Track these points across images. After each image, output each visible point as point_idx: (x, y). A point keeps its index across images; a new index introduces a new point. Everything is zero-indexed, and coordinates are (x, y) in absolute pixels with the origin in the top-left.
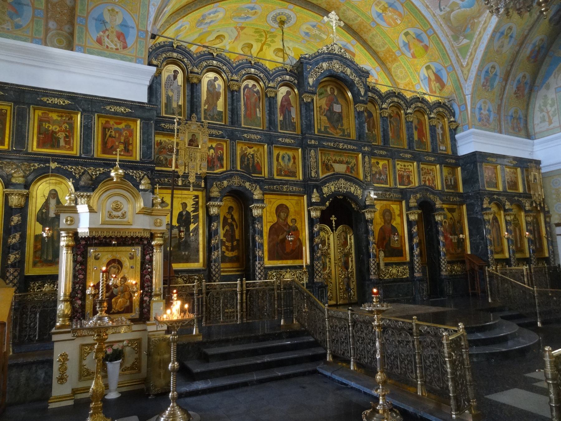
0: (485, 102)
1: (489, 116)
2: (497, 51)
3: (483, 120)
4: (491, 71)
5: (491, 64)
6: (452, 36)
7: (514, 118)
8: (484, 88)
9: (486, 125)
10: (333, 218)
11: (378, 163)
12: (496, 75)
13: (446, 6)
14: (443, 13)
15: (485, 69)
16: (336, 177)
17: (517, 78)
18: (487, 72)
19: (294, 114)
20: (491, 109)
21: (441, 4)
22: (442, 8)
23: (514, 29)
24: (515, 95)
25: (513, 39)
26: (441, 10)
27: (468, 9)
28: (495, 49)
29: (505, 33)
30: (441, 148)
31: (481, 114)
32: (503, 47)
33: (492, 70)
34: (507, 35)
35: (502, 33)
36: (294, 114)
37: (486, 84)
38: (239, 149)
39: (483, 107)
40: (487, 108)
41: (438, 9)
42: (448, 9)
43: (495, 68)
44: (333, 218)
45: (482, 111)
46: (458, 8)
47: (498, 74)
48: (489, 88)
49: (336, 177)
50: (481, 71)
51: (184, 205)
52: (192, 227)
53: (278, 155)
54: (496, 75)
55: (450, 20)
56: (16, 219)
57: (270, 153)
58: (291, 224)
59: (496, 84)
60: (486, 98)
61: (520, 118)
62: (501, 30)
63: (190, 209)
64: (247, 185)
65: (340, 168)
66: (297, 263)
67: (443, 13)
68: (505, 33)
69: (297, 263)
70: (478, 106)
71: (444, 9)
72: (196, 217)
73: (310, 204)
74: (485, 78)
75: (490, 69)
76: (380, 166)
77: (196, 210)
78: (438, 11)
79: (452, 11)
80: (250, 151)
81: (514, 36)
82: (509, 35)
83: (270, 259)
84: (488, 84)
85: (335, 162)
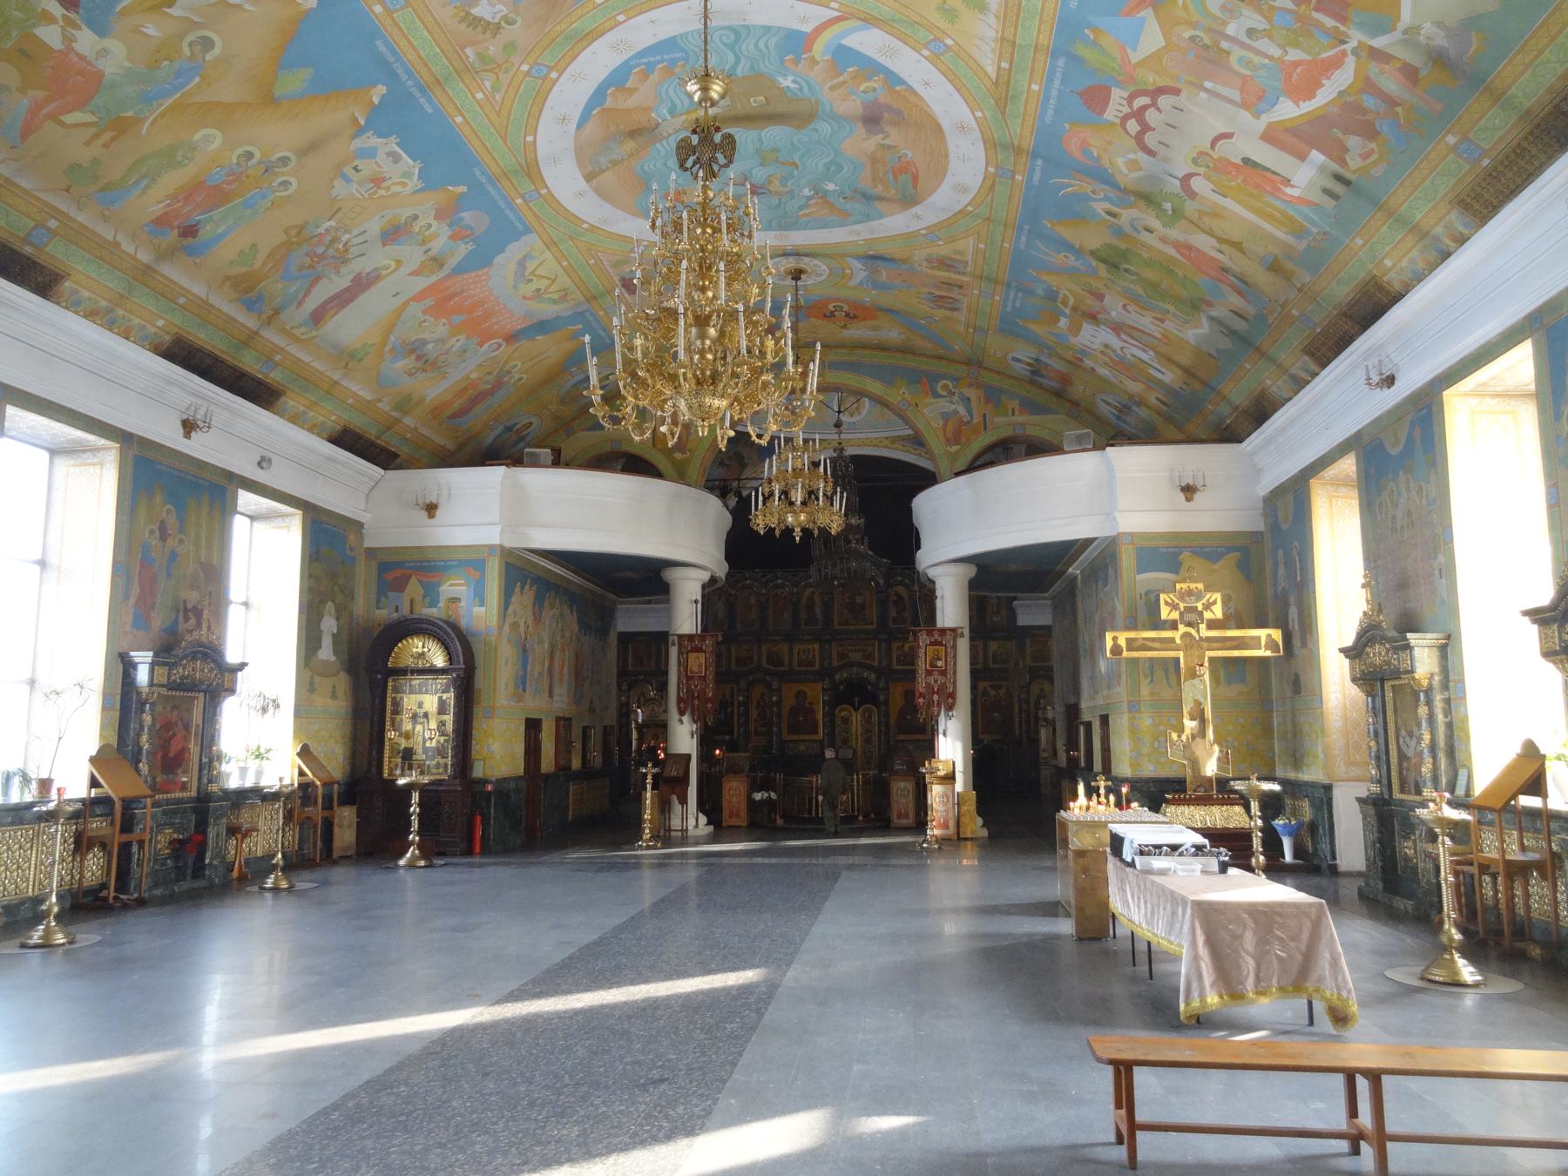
10: (857, 699)
11: (903, 646)
16: (851, 665)
19: (818, 611)
30: (995, 619)
36: (818, 611)
38: (764, 648)
44: (857, 699)
49: (851, 665)
51: (724, 695)
52: (729, 710)
53: (799, 650)
56: (624, 709)
57: (791, 649)
58: (808, 706)
63: (728, 697)
64: (768, 678)
65: (856, 657)
66: (814, 737)
69: (814, 737)
72: (732, 704)
73: (824, 690)
76: (906, 648)
77: (732, 697)
80: (775, 649)
83: (817, 733)
85: (851, 651)
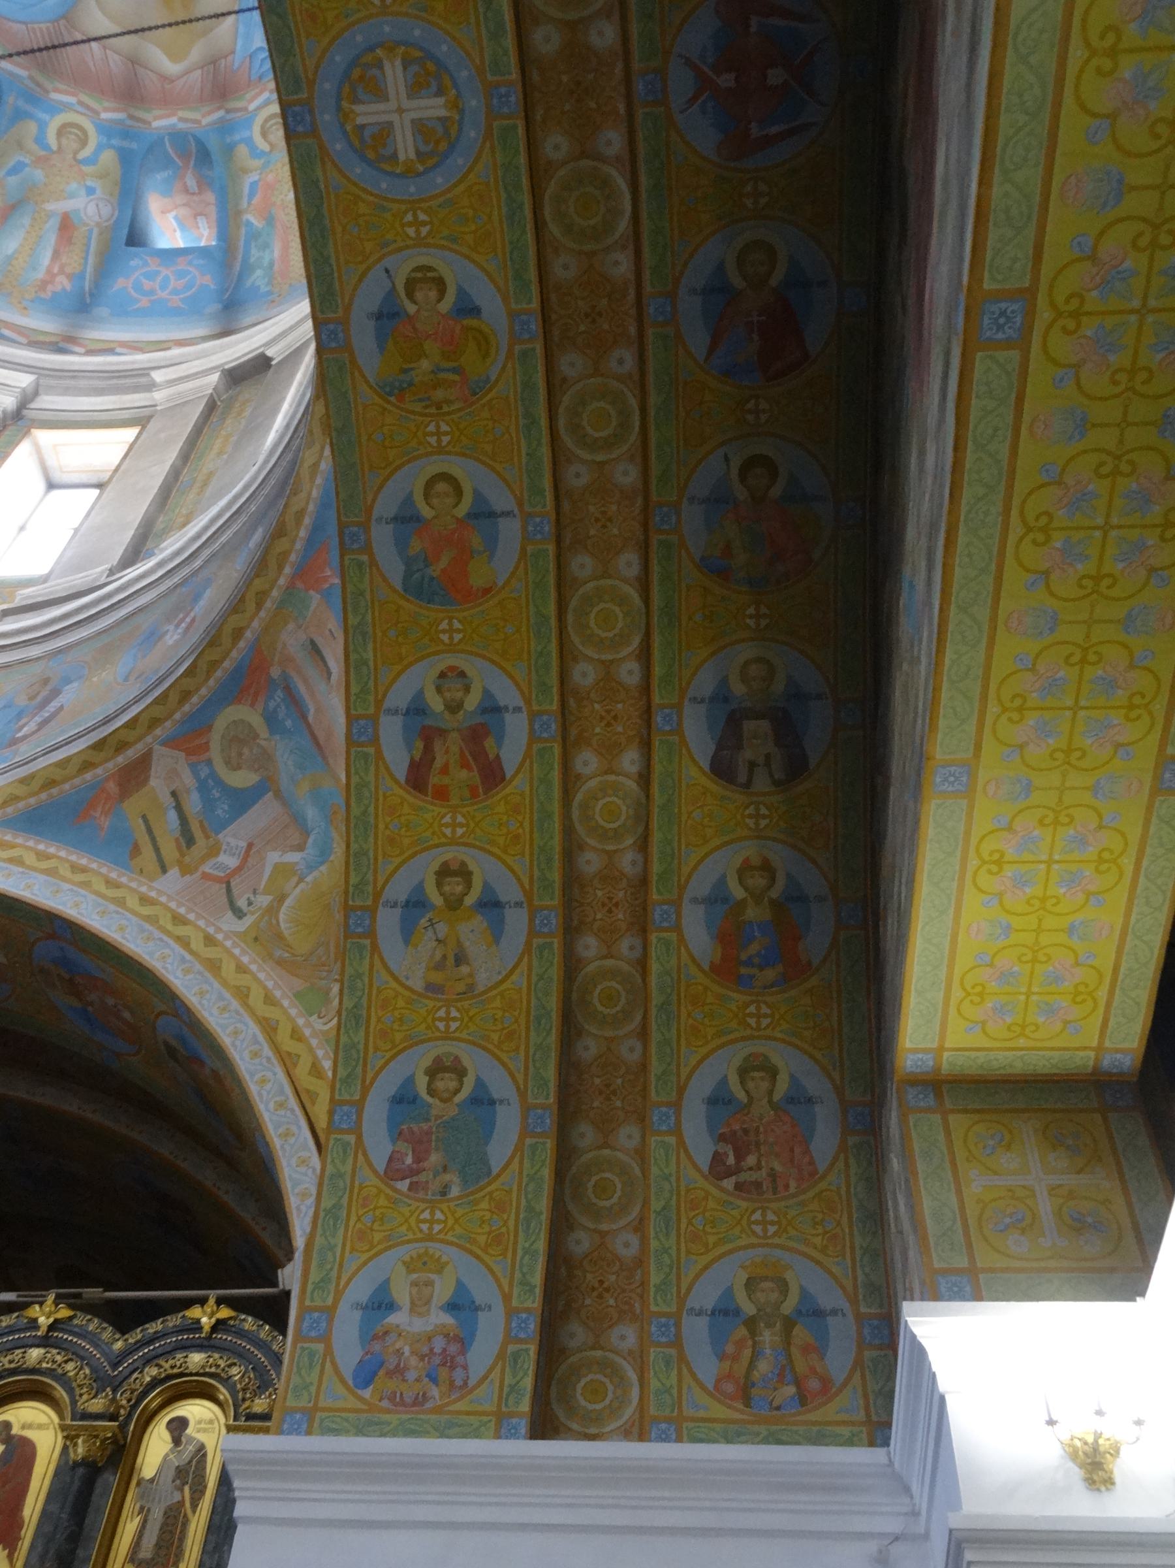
0: (420, 1264)
1: (463, 1341)
2: (432, 988)
3: (399, 1371)
4: (431, 1092)
5: (417, 1063)
6: (298, 995)
7: (751, 1324)
8: (403, 1185)
9: (420, 1401)
12: (482, 1100)
13: (255, 892)
14: (249, 920)
15: (386, 1086)
17: (701, 1087)
18: (404, 1099)
20: (483, 1290)
21: (235, 891)
22: (242, 903)
23: (483, 868)
24: (728, 1184)
25: (510, 914)
26: (239, 914)
27: (323, 868)
28: (418, 984)
29: (436, 899)
31: (373, 1335)
32: (460, 959)
33: (446, 1083)
34: (454, 904)
35: (416, 904)
37: (418, 1159)
39: (402, 1293)
40: (443, 1290)
41: (230, 914)
42: (264, 900)
43: (460, 1072)
45: (393, 1319)
46: (295, 879)
47: (500, 1085)
48: (452, 1177)
50: (359, 1105)
54: (482, 1100)
55: (280, 936)
59: (500, 1149)
60: (430, 1238)
61: (815, 1313)
62: (398, 891)
67: (249, 920)
68: (436, 899)
70: (360, 1290)
71: (250, 904)
74: (397, 1135)
75: (422, 1082)
78: (229, 922)
79: (282, 898)
81: (509, 891)
82: (469, 900)
84: (434, 1158)
